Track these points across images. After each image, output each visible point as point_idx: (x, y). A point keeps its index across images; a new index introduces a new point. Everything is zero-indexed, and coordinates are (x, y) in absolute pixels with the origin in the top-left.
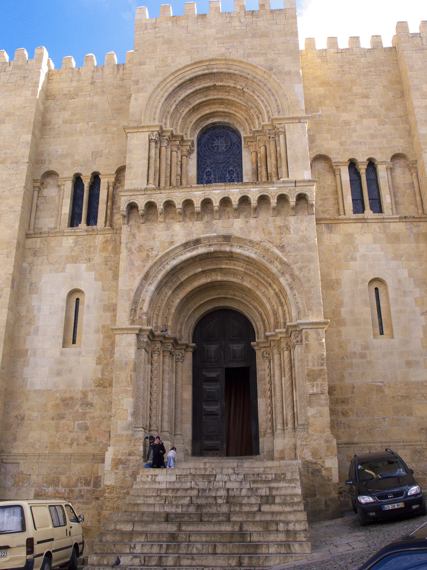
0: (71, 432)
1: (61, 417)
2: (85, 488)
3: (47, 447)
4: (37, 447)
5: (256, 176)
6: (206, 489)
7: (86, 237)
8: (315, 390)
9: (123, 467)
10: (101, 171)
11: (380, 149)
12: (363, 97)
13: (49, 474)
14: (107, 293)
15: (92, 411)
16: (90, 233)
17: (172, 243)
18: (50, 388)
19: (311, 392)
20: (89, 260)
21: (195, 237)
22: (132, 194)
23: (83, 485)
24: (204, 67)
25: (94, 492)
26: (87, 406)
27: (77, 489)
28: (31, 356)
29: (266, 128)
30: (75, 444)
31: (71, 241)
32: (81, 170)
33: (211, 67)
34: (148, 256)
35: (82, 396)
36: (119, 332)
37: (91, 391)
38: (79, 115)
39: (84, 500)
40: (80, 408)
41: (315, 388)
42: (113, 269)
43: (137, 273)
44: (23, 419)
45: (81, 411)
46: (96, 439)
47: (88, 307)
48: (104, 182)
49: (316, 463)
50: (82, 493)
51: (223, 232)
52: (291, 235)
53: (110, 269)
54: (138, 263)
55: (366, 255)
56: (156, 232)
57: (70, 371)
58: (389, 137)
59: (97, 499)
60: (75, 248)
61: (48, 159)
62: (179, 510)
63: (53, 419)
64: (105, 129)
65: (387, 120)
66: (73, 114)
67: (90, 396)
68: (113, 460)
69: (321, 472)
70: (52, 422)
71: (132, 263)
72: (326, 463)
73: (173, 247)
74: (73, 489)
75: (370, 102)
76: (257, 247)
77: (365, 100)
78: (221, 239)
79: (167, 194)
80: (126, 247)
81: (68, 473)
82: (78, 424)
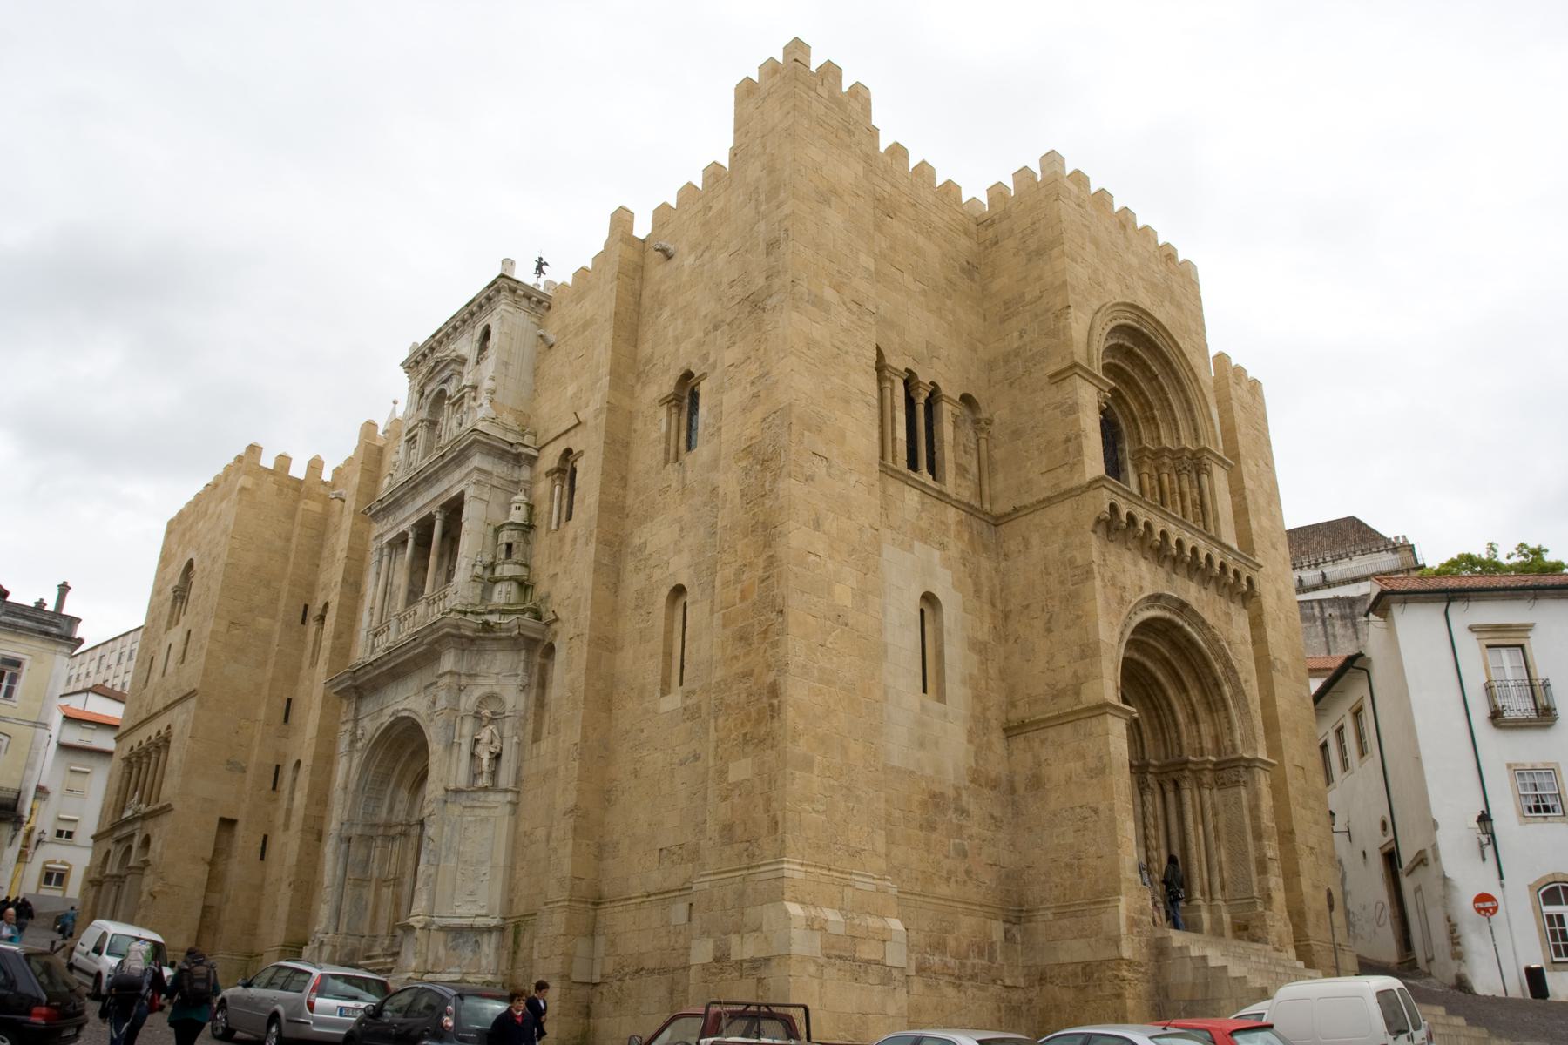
1: (932, 827)
4: (905, 878)
7: (934, 500)
10: (941, 385)
13: (932, 931)
14: (970, 617)
16: (942, 497)
18: (912, 769)
20: (943, 546)
21: (1160, 590)
22: (1115, 489)
24: (1135, 317)
25: (989, 969)
26: (962, 815)
27: (969, 963)
29: (1187, 453)
30: (953, 879)
33: (1140, 320)
35: (955, 795)
37: (967, 788)
40: (954, 816)
42: (974, 576)
43: (1114, 620)
45: (955, 821)
47: (950, 634)
48: (946, 411)
53: (970, 577)
54: (1114, 605)
59: (994, 981)
60: (923, 514)
63: (921, 827)
66: (892, 248)
68: (1128, 917)
70: (920, 833)
73: (1143, 596)
74: (965, 961)
76: (1206, 632)
81: (956, 932)
82: (954, 844)
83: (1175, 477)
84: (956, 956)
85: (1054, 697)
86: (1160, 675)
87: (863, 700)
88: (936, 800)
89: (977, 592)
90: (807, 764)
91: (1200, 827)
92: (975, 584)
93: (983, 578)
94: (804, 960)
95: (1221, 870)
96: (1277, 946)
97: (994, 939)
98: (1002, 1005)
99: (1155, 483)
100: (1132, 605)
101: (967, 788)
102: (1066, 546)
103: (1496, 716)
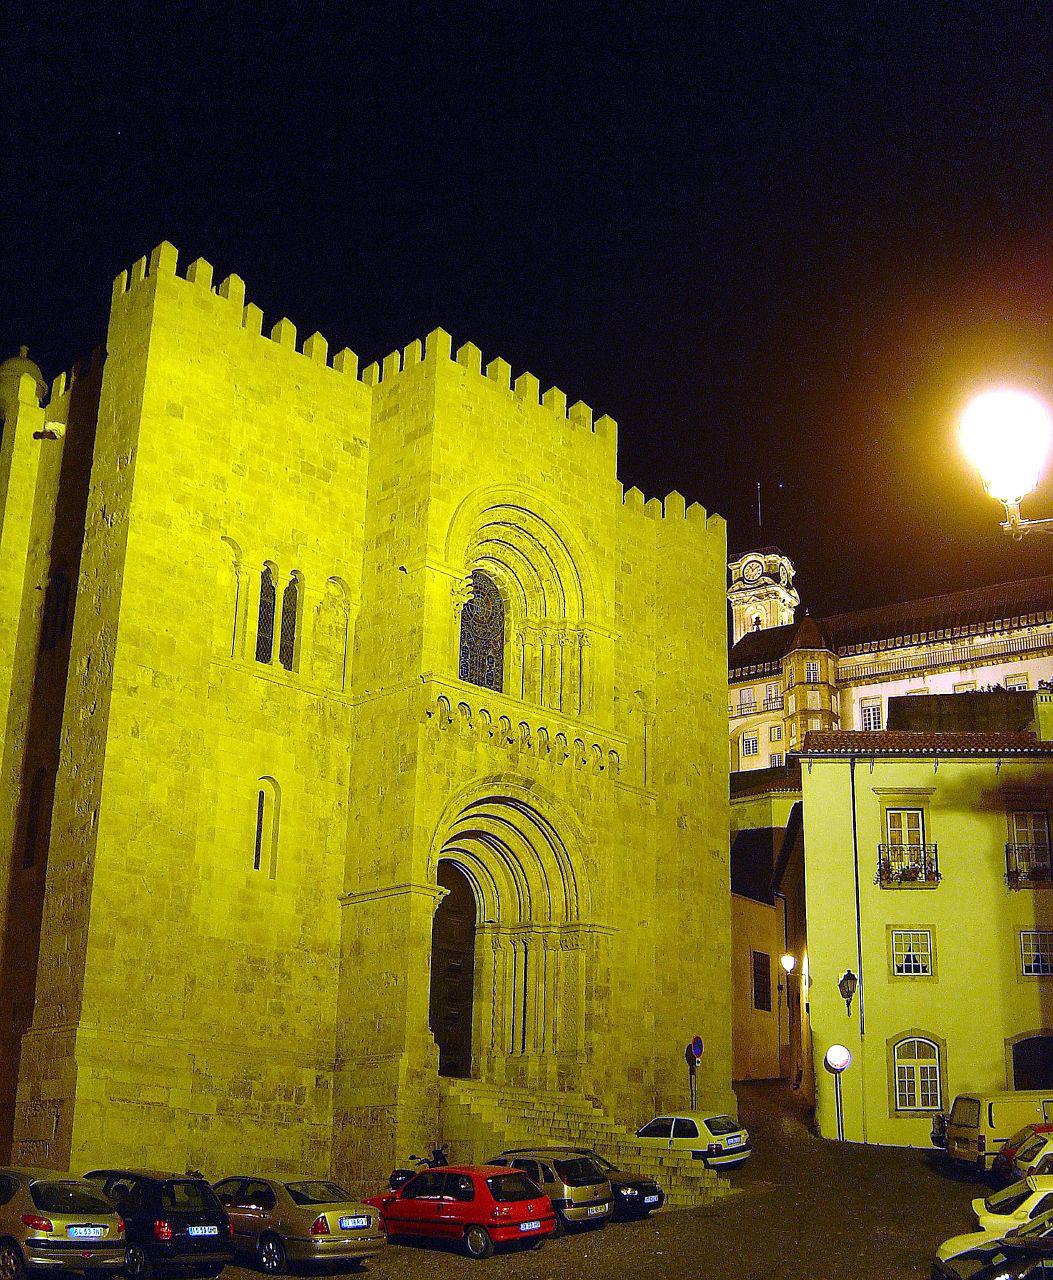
1: (248, 989)
10: (304, 572)
25: (296, 1110)
27: (274, 1104)
31: (262, 689)
36: (418, 889)
38: (273, 445)
47: (285, 813)
53: (317, 757)
54: (437, 791)
83: (558, 648)
84: (262, 1098)
85: (378, 872)
86: (515, 842)
87: (170, 884)
88: (256, 965)
89: (324, 774)
90: (108, 942)
91: (542, 985)
92: (322, 764)
93: (332, 759)
94: (87, 1102)
95: (555, 1025)
96: (592, 1093)
97: (304, 1085)
98: (307, 1140)
99: (538, 654)
100: (459, 789)
102: (401, 733)
103: (885, 875)
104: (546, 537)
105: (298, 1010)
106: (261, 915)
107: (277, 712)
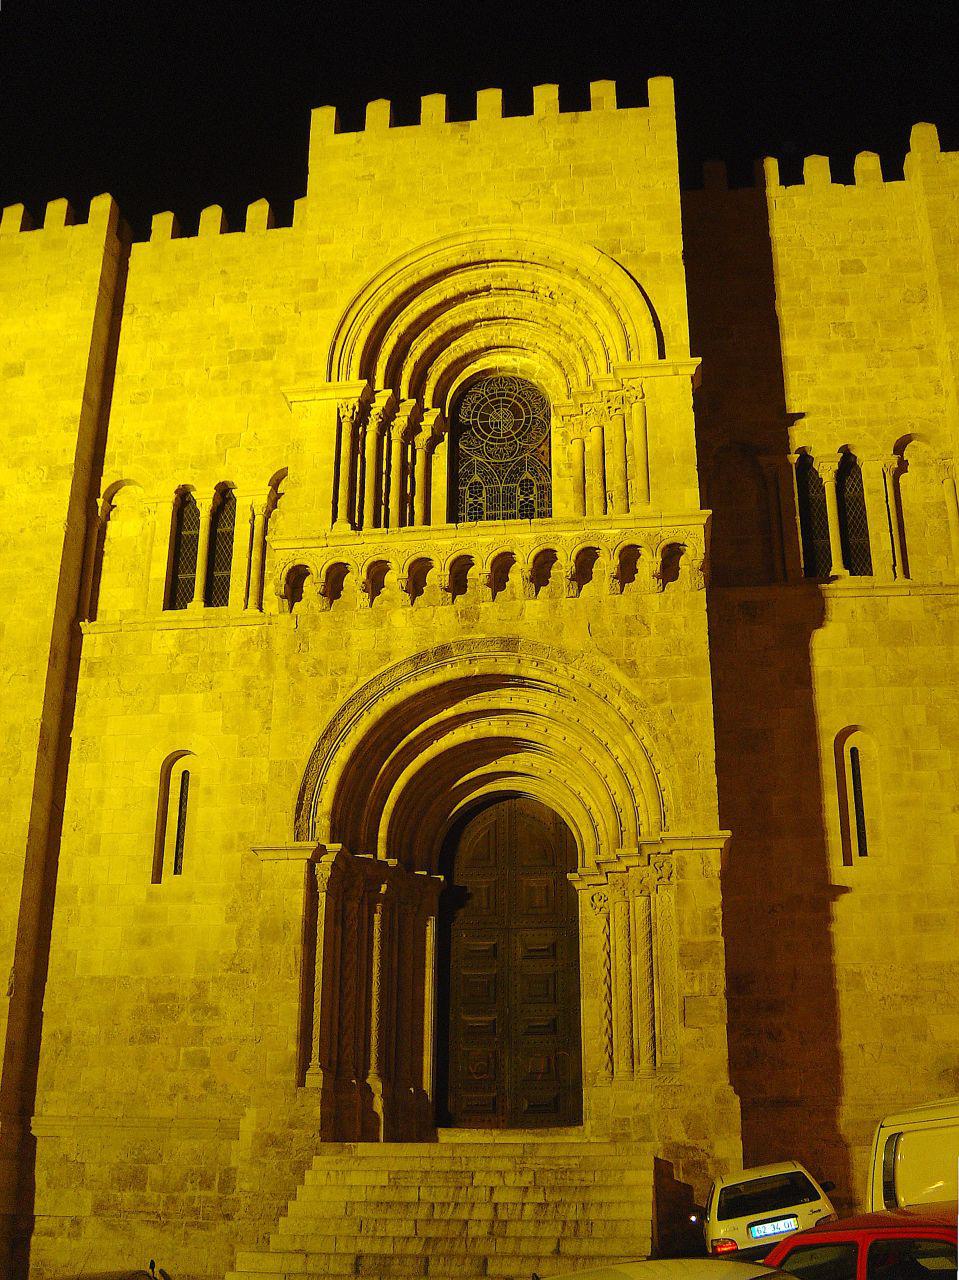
0: (171, 1070)
1: (149, 1037)
2: (203, 1193)
3: (118, 1103)
5: (581, 496)
6: (449, 1204)
8: (697, 988)
9: (278, 1153)
11: (870, 424)
12: (834, 302)
15: (216, 1023)
17: (387, 655)
18: (125, 974)
19: (688, 991)
21: (437, 641)
23: (198, 1187)
25: (220, 1202)
26: (206, 1012)
27: (184, 1196)
28: (83, 902)
30: (180, 1096)
31: (171, 642)
32: (193, 479)
34: (335, 684)
37: (215, 980)
39: (200, 1220)
41: (697, 983)
44: (67, 1039)
45: (191, 1023)
46: (225, 1086)
47: (208, 791)
49: (694, 1149)
50: (195, 1205)
51: (504, 632)
52: (651, 638)
54: (312, 701)
55: (830, 672)
56: (353, 632)
57: (169, 935)
58: (892, 395)
61: (120, 453)
62: (388, 1250)
64: (247, 383)
65: (888, 355)
67: (212, 991)
68: (256, 1136)
69: (706, 1169)
71: (299, 702)
72: (715, 1148)
74: (176, 1194)
75: (849, 314)
77: (838, 306)
78: (496, 647)
79: (375, 546)
80: (287, 666)
81: (165, 1160)
82: (186, 1054)
84: (163, 1188)
97: (233, 1164)
101: (215, 980)
104: (549, 279)
105: (232, 1057)
106: (169, 935)
107: (195, 666)
